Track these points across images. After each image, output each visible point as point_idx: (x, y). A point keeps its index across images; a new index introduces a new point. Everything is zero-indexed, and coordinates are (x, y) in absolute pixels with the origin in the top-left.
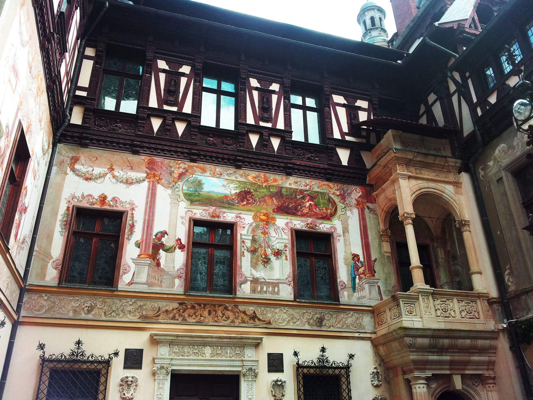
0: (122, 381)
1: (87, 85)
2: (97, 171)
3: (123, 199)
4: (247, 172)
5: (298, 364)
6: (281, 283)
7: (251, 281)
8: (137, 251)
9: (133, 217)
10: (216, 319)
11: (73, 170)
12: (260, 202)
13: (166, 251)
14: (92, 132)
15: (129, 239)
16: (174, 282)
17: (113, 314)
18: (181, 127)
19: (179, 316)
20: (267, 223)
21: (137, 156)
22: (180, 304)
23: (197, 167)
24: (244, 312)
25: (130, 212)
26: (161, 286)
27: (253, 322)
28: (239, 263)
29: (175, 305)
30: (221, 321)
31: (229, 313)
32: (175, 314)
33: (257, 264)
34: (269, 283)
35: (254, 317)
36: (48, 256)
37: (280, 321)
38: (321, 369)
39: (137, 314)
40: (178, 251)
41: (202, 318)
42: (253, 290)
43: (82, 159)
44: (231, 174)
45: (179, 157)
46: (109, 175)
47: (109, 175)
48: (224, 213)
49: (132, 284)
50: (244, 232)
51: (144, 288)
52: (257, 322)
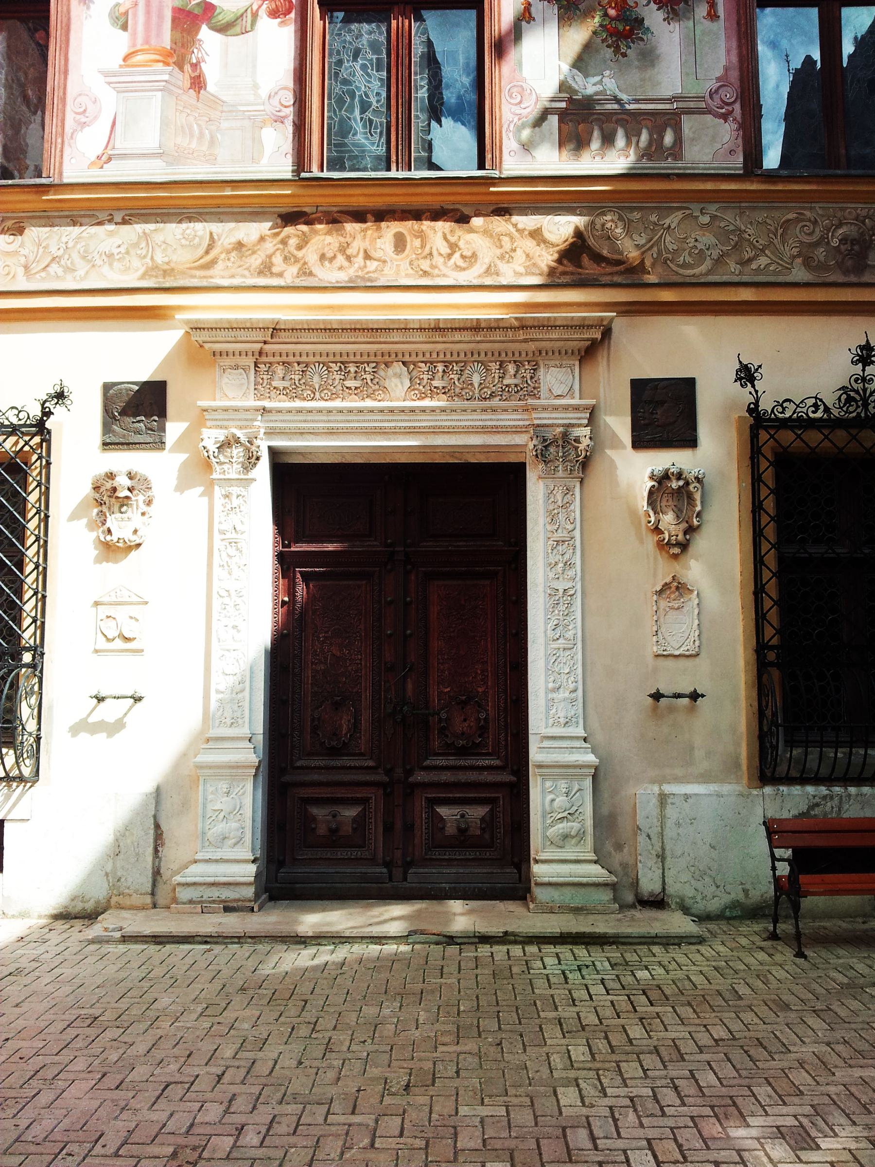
0: (96, 488)
5: (753, 410)
6: (690, 112)
8: (121, 42)
10: (425, 265)
13: (223, 29)
16: (257, 141)
17: (54, 267)
19: (286, 259)
26: (212, 159)
27: (571, 268)
30: (445, 270)
32: (270, 257)
34: (636, 115)
37: (684, 258)
38: (854, 432)
39: (136, 263)
40: (266, 23)
41: (372, 265)
49: (110, 159)
52: (590, 268)
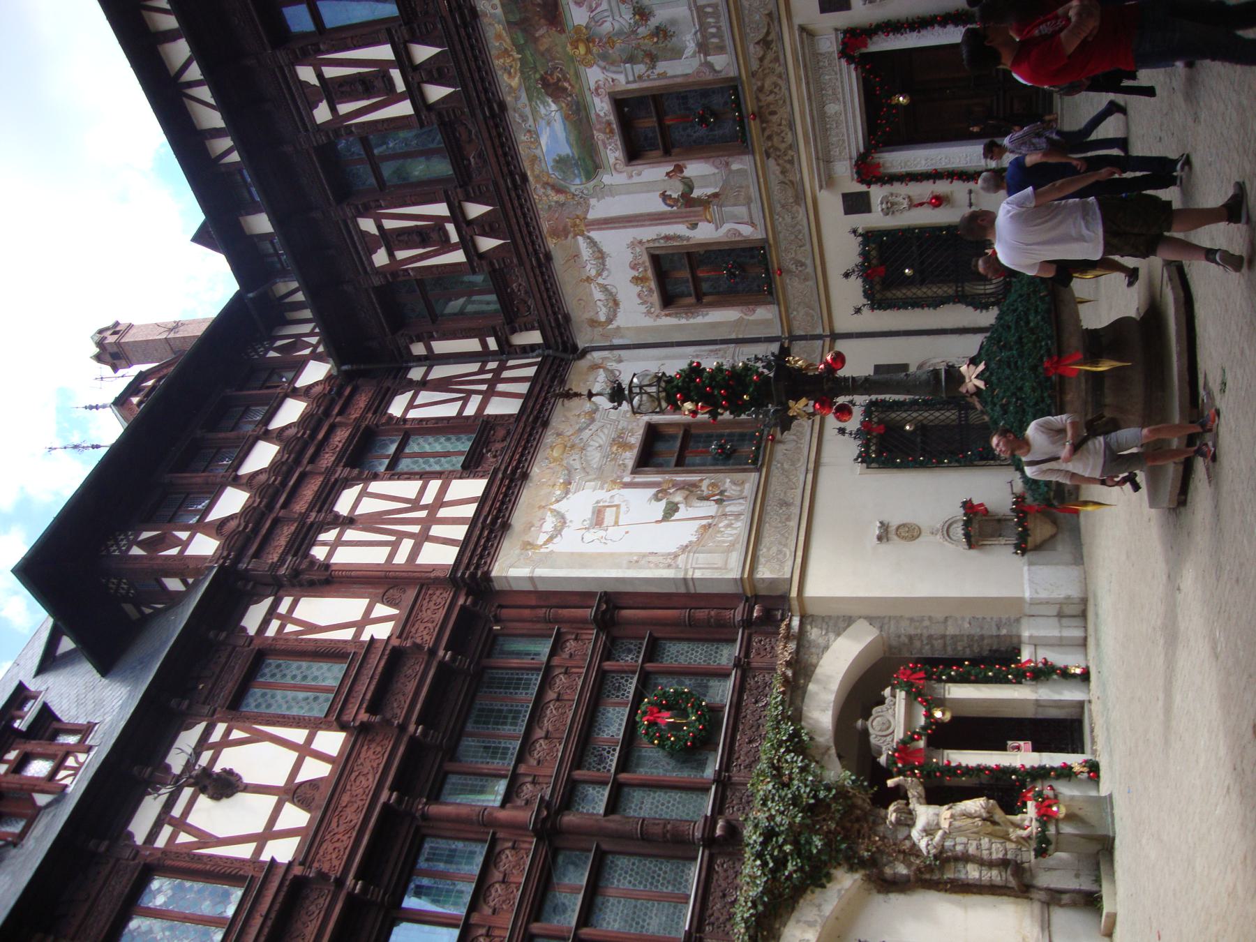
1: (477, 340)
2: (598, 295)
3: (630, 258)
4: (505, 89)
7: (706, 55)
9: (654, 240)
11: (610, 321)
12: (553, 59)
13: (691, 189)
14: (544, 316)
15: (688, 239)
18: (475, 210)
20: (589, 40)
21: (553, 253)
22: (768, 156)
23: (533, 170)
24: (761, 59)
25: (647, 245)
26: (748, 187)
28: (679, 80)
29: (771, 162)
31: (768, 83)
33: (673, 50)
34: (701, 24)
35: (765, 43)
36: (740, 321)
40: (687, 173)
41: (784, 122)
42: (721, 49)
43: (587, 316)
44: (521, 116)
45: (529, 198)
46: (600, 280)
47: (600, 280)
48: (598, 115)
50: (621, 78)
51: (756, 207)
52: (772, 36)
